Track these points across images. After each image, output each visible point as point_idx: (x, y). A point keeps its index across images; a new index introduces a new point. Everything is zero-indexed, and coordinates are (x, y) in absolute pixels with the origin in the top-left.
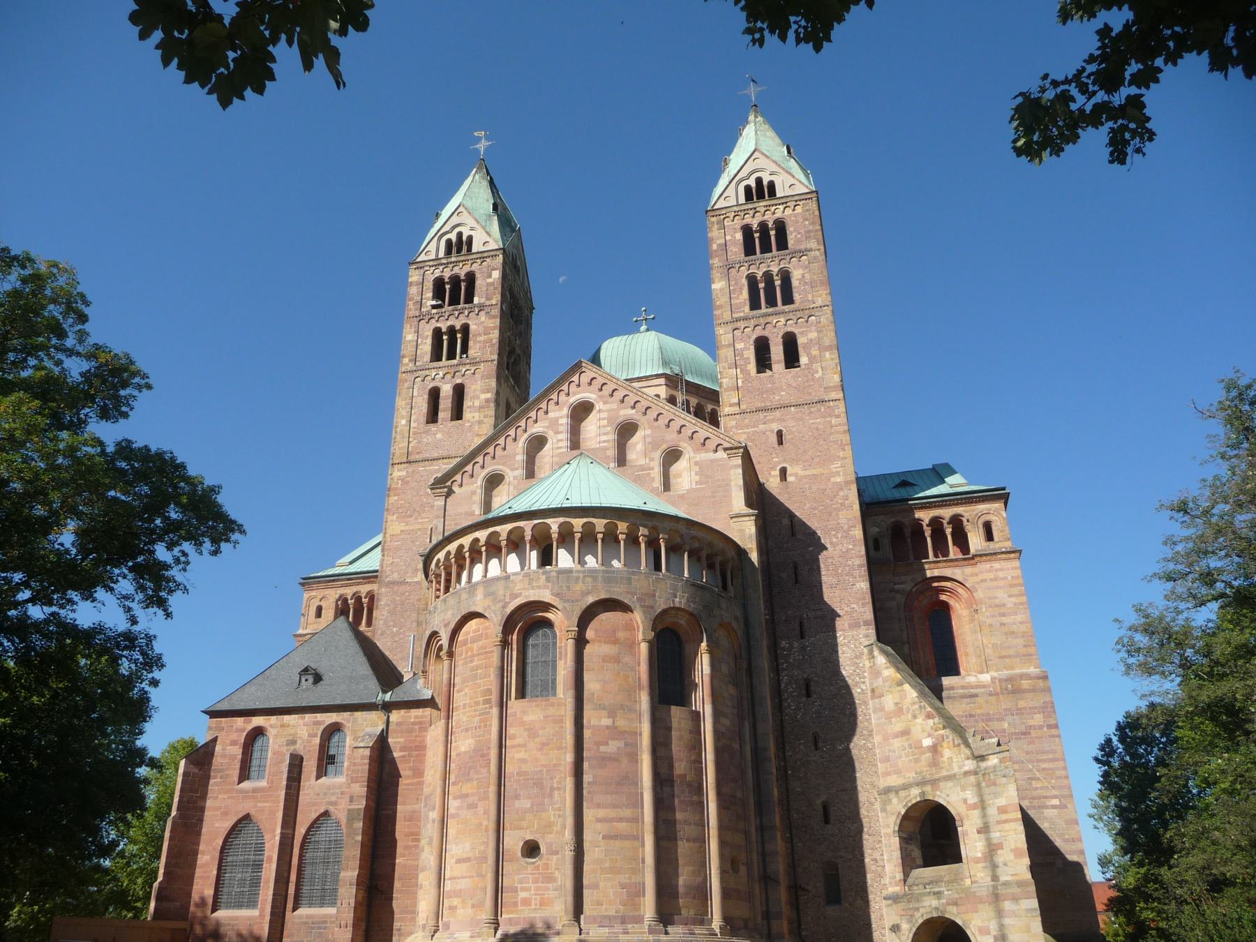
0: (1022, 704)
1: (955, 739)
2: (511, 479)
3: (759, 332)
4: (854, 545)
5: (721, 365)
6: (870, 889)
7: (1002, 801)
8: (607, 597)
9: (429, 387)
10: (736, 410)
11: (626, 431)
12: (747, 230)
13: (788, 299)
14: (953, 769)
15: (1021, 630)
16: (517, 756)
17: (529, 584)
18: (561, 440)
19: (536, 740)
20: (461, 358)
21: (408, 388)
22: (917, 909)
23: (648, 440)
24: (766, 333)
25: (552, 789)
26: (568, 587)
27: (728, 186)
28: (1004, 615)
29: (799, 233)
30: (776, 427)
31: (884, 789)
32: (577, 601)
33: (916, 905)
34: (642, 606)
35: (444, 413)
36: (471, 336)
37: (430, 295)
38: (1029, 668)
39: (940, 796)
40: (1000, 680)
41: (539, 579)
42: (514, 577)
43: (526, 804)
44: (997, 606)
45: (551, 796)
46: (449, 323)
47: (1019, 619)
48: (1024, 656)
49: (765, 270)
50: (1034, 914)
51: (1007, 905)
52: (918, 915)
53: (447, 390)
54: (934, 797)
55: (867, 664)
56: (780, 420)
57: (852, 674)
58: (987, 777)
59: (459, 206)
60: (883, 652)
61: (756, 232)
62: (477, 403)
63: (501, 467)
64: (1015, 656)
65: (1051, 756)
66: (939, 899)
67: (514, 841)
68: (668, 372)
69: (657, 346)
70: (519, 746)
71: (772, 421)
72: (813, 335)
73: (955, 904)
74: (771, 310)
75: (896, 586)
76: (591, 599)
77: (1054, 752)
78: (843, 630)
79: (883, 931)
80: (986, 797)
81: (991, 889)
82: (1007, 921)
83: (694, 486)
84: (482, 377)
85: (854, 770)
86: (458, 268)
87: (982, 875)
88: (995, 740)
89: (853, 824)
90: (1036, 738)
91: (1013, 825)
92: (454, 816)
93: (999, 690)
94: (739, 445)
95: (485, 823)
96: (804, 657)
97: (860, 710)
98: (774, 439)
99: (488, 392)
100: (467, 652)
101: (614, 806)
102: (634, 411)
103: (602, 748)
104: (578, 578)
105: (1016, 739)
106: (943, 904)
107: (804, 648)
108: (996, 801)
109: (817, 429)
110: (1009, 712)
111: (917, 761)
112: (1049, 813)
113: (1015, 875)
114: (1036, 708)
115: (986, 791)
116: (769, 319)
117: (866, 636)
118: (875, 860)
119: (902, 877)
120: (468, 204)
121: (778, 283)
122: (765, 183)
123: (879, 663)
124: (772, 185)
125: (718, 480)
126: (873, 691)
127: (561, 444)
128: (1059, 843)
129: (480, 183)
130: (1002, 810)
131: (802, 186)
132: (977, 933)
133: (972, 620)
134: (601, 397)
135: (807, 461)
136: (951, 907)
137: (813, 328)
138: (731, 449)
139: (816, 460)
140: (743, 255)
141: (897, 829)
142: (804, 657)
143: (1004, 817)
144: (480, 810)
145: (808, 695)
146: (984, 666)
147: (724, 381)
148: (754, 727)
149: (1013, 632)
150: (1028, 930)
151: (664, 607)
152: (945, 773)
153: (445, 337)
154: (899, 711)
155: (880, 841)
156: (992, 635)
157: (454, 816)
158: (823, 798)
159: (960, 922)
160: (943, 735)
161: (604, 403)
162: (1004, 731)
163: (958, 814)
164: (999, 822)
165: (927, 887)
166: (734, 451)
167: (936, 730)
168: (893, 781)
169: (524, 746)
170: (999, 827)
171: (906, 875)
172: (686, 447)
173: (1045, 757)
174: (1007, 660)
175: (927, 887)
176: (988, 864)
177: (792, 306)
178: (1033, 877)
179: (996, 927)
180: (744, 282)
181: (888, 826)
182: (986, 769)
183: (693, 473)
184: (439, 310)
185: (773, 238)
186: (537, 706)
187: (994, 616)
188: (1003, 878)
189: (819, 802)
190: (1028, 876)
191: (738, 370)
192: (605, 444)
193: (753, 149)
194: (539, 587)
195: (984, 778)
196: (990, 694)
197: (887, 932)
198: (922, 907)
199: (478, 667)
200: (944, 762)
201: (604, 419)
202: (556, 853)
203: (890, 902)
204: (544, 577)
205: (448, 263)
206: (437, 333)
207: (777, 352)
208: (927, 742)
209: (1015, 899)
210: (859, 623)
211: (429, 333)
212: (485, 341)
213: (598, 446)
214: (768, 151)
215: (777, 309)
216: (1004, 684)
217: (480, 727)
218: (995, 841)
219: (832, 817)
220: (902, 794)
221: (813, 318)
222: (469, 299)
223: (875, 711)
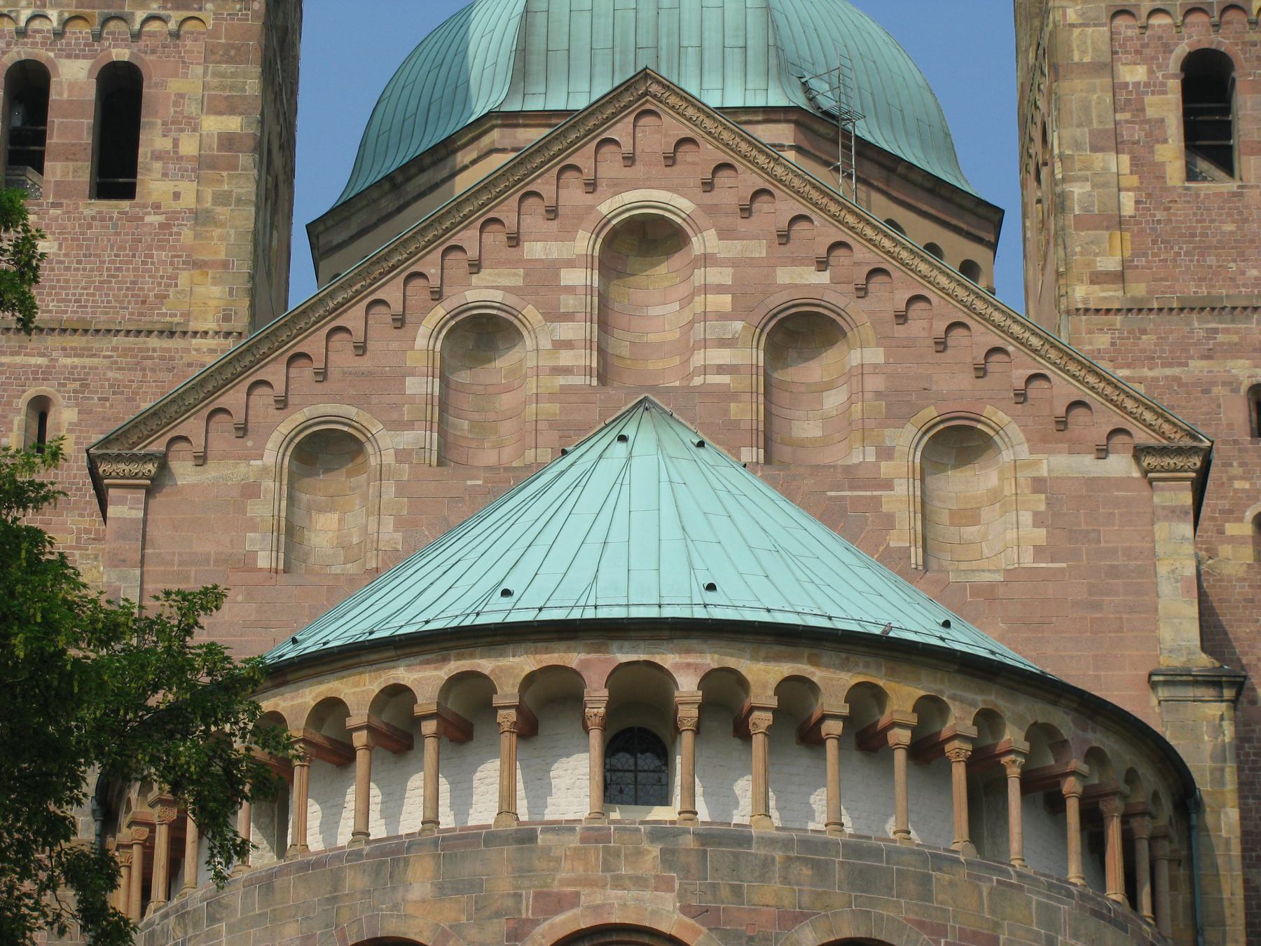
2: (389, 458)
3: (1197, 36)
5: (1064, 133)
8: (862, 933)
10: (1109, 295)
17: (607, 867)
18: (568, 345)
23: (875, 383)
24: (1223, 42)
26: (737, 891)
41: (639, 853)
42: (549, 836)
62: (189, 146)
63: (351, 411)
68: (800, 101)
71: (1235, 351)
83: (1028, 560)
84: (210, 51)
94: (1188, 442)
99: (232, 111)
102: (824, 278)
104: (766, 863)
127: (566, 358)
134: (712, 210)
138: (1162, 451)
147: (1077, 191)
161: (724, 234)
172: (997, 416)
183: (1027, 518)
191: (1125, 159)
192: (725, 379)
194: (640, 882)
201: (720, 289)
204: (655, 850)
213: (698, 381)
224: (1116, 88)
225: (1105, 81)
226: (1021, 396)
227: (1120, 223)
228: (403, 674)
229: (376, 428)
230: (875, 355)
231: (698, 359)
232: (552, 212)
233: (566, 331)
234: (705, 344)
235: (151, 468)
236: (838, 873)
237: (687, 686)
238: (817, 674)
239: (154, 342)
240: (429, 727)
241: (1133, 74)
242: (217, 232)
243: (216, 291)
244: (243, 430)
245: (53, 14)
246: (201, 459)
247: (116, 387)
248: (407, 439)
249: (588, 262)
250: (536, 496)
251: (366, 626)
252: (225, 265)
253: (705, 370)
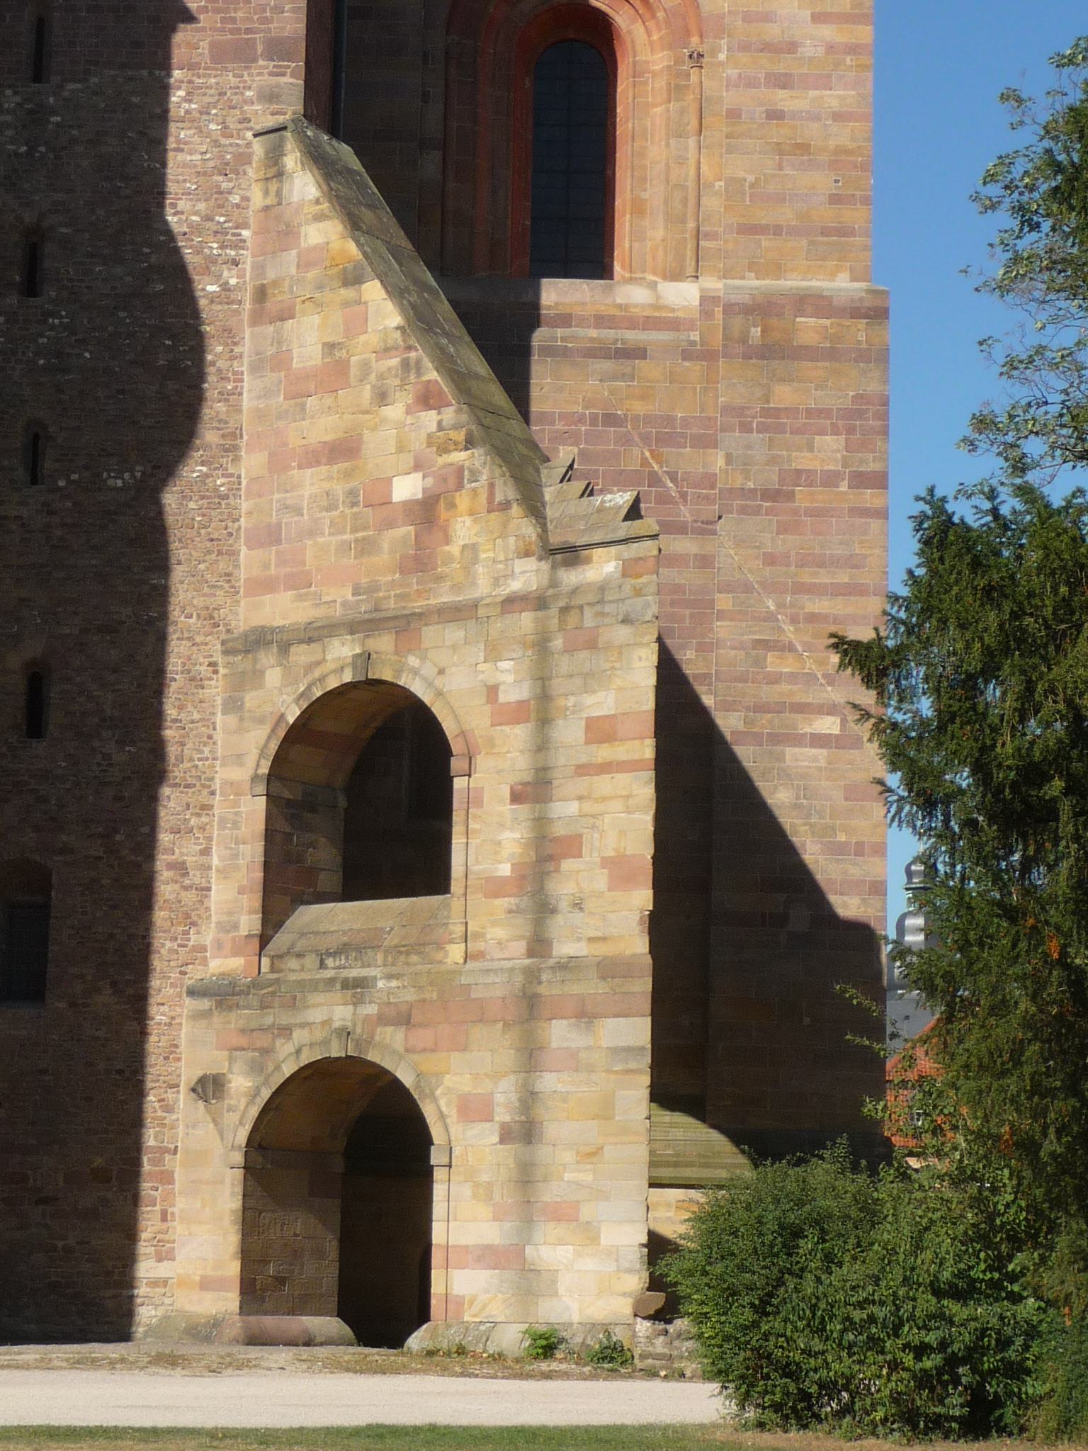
0: (784, 395)
1: (499, 483)
6: (157, 963)
7: (602, 703)
14: (473, 584)
15: (832, 143)
22: (286, 1031)
28: (784, 82)
31: (246, 635)
33: (285, 1019)
38: (832, 276)
39: (415, 672)
40: (729, 309)
44: (767, 47)
47: (835, 104)
48: (825, 232)
50: (633, 1065)
51: (559, 1034)
52: (284, 1048)
54: (398, 672)
55: (257, 198)
57: (196, 229)
58: (572, 619)
60: (317, 159)
64: (794, 232)
65: (843, 577)
66: (357, 1001)
73: (404, 1019)
77: (853, 563)
78: (192, 67)
79: (170, 1095)
80: (558, 685)
81: (519, 979)
82: (549, 1082)
85: (161, 564)
87: (498, 933)
88: (623, 499)
89: (121, 743)
90: (811, 513)
91: (623, 779)
93: (717, 341)
96: (32, 149)
97: (215, 352)
105: (743, 510)
106: (367, 1018)
108: (589, 700)
110: (740, 418)
111: (365, 547)
112: (800, 758)
113: (604, 939)
114: (825, 413)
115: (563, 664)
117: (270, 96)
118: (181, 868)
119: (257, 928)
123: (295, 198)
126: (261, 294)
128: (812, 854)
130: (600, 731)
132: (451, 1111)
133: (676, 90)
136: (390, 1029)
141: (264, 769)
142: (32, 149)
143: (604, 753)
145: (31, 287)
146: (690, 253)
149: (804, 148)
150: (605, 1111)
155: (206, 808)
156: (730, 150)
158: (33, 648)
159: (407, 1079)
160: (460, 470)
162: (709, 480)
163: (463, 734)
164: (584, 770)
165: (330, 962)
167: (443, 450)
170: (582, 784)
171: (272, 919)
173: (824, 578)
174: (766, 242)
175: (330, 962)
176: (525, 902)
178: (652, 951)
179: (514, 1097)
181: (239, 759)
182: (575, 591)
187: (751, 83)
188: (565, 948)
189: (15, 661)
190: (638, 945)
195: (562, 621)
196: (687, 355)
197: (182, 1098)
198: (302, 1026)
200: (449, 559)
203: (205, 1004)
208: (407, 488)
209: (585, 1015)
210: (250, 44)
216: (737, 322)
218: (559, 830)
219: (55, 718)
220: (301, 654)
223: (255, 369)
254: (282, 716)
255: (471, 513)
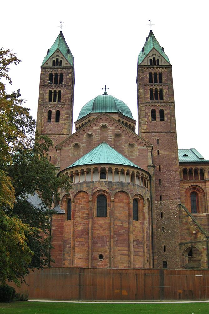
2: (81, 147)
4: (177, 176)
9: (48, 110)
10: (145, 131)
11: (118, 135)
12: (150, 74)
13: (161, 99)
16: (96, 232)
18: (97, 137)
19: (102, 228)
20: (58, 102)
21: (41, 110)
23: (124, 140)
24: (155, 108)
25: (107, 242)
27: (145, 58)
29: (166, 78)
30: (156, 138)
32: (114, 191)
34: (130, 193)
35: (53, 120)
36: (62, 95)
37: (48, 79)
39: (196, 246)
43: (100, 245)
45: (106, 243)
46: (54, 89)
49: (155, 88)
53: (54, 112)
54: (195, 246)
56: (158, 136)
59: (57, 49)
61: (153, 75)
62: (64, 118)
63: (78, 143)
67: (96, 255)
69: (114, 102)
70: (97, 229)
71: (156, 136)
72: (168, 111)
74: (156, 101)
75: (184, 187)
76: (117, 191)
84: (65, 109)
86: (57, 71)
89: (172, 252)
92: (76, 247)
95: (87, 249)
98: (156, 142)
100: (80, 202)
101: (123, 247)
102: (120, 131)
103: (120, 232)
104: (114, 184)
107: (161, 204)
109: (169, 140)
116: (156, 104)
117: (179, 202)
120: (60, 49)
121: (159, 93)
122: (156, 59)
124: (158, 60)
125: (144, 155)
126: (179, 217)
127: (97, 138)
129: (62, 41)
131: (167, 62)
134: (110, 124)
135: (165, 149)
137: (169, 109)
138: (149, 146)
139: (168, 149)
140: (149, 82)
144: (86, 246)
145: (162, 217)
147: (142, 121)
148: (152, 226)
151: (135, 194)
152: (198, 241)
153: (53, 94)
154: (187, 223)
157: (76, 247)
158: (164, 245)
166: (149, 147)
168: (183, 241)
169: (99, 229)
172: (135, 143)
177: (163, 101)
180: (149, 90)
181: (181, 253)
183: (137, 152)
184: (51, 85)
185: (158, 78)
186: (102, 219)
189: (163, 246)
193: (152, 47)
194: (103, 186)
196: (206, 219)
199: (83, 207)
201: (111, 132)
202: (108, 258)
204: (104, 183)
205: (54, 69)
206: (50, 92)
207: (158, 115)
208: (194, 232)
211: (48, 92)
212: (66, 97)
214: (157, 48)
215: (158, 101)
217: (85, 223)
219: (166, 250)
220: (186, 245)
221: (169, 106)
222: (61, 82)
224: (146, 112)
225: (144, 112)
226: (136, 141)
227: (146, 124)
228: (83, 168)
229: (80, 144)
230: (124, 138)
231: (109, 138)
232: (95, 125)
233: (97, 135)
234: (109, 137)
235: (61, 148)
236: (120, 185)
237: (107, 169)
238: (118, 168)
239: (61, 135)
240: (85, 173)
241: (147, 111)
242: (66, 125)
243: (66, 131)
244: (69, 144)
245: (52, 106)
246: (65, 147)
247: (58, 139)
248: (83, 145)
249: (99, 129)
250: (94, 151)
251: (79, 163)
252: (67, 128)
253: (109, 139)
254: (184, 250)
255: (200, 234)
